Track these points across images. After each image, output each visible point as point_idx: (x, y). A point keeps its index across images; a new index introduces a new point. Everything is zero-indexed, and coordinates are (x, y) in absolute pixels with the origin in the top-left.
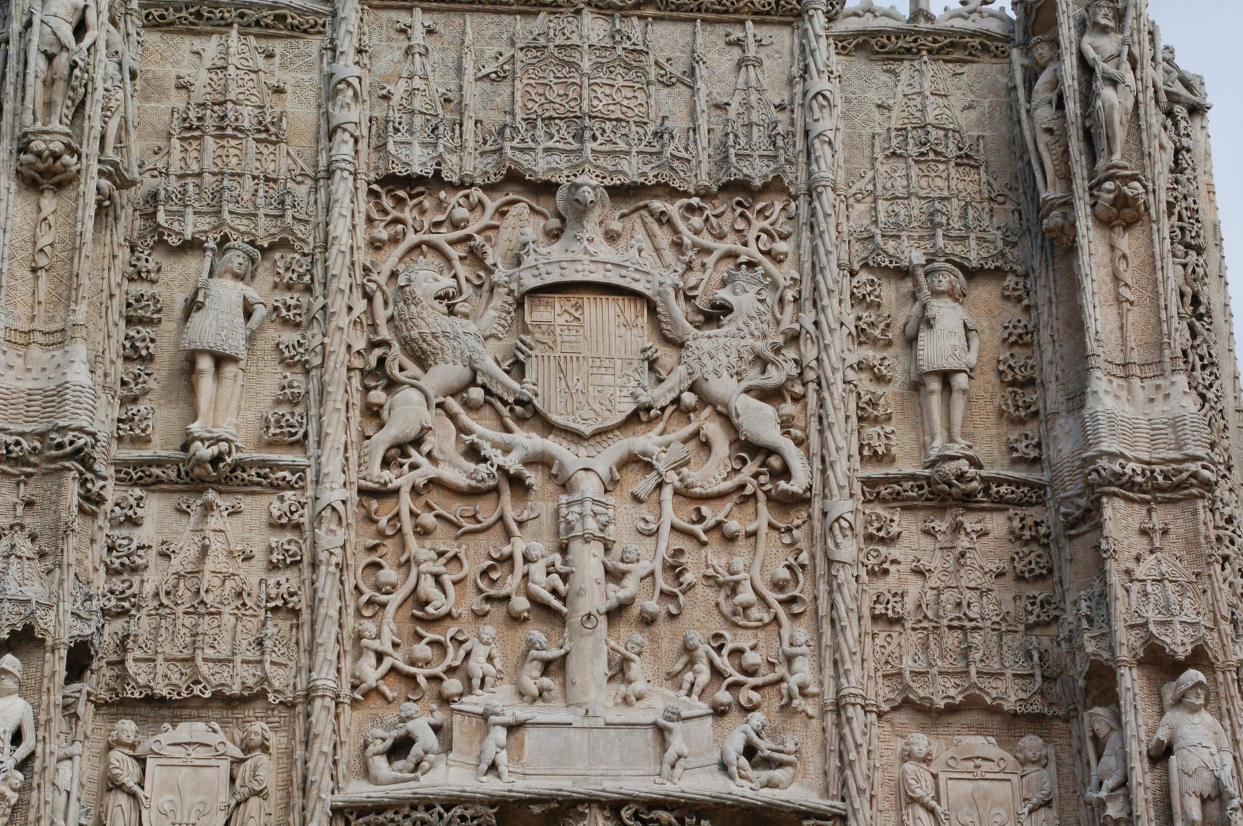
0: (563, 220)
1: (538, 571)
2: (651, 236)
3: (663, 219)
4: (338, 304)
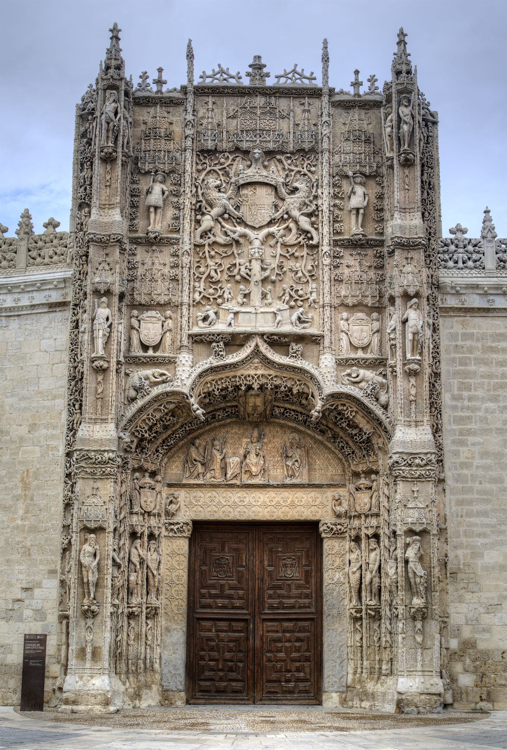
0: (251, 162)
1: (243, 269)
2: (277, 166)
3: (280, 161)
4: (188, 190)
